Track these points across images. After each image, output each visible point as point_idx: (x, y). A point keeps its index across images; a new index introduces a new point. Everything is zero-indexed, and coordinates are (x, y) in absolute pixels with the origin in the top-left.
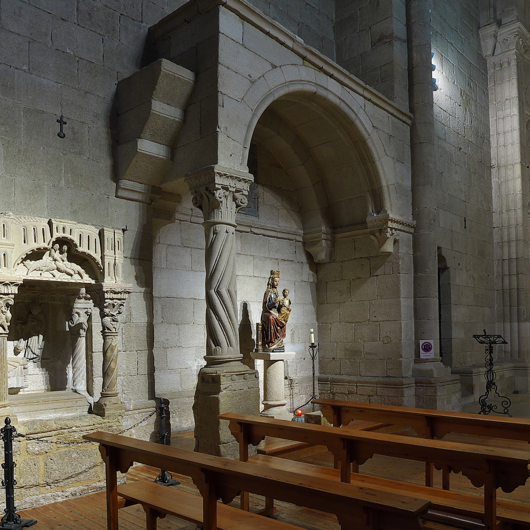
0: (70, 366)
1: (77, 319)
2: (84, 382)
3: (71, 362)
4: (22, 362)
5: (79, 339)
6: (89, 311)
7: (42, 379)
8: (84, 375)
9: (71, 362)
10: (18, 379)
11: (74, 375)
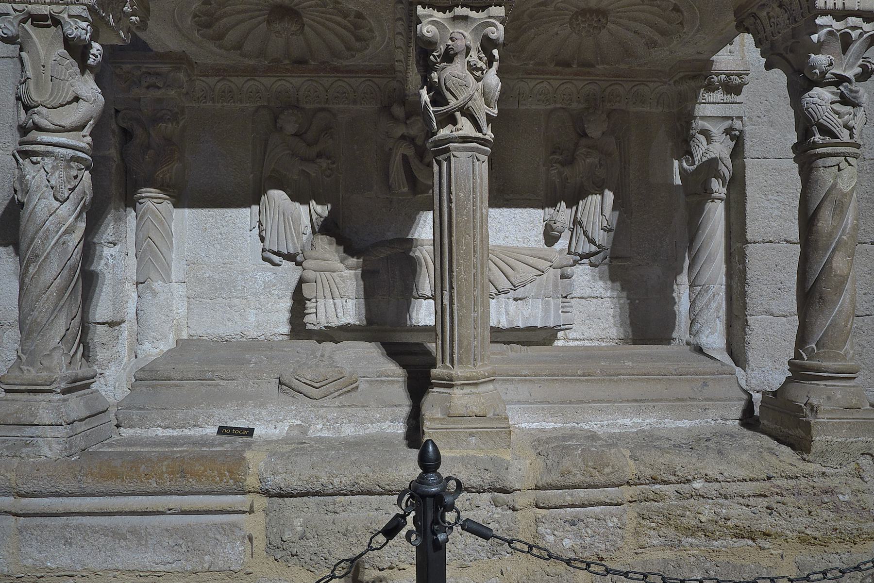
0: (683, 278)
1: (702, 150)
2: (720, 326)
3: (686, 270)
4: (557, 259)
5: (709, 205)
6: (738, 124)
7: (611, 311)
8: (720, 305)
9: (686, 270)
10: (548, 303)
11: (693, 303)
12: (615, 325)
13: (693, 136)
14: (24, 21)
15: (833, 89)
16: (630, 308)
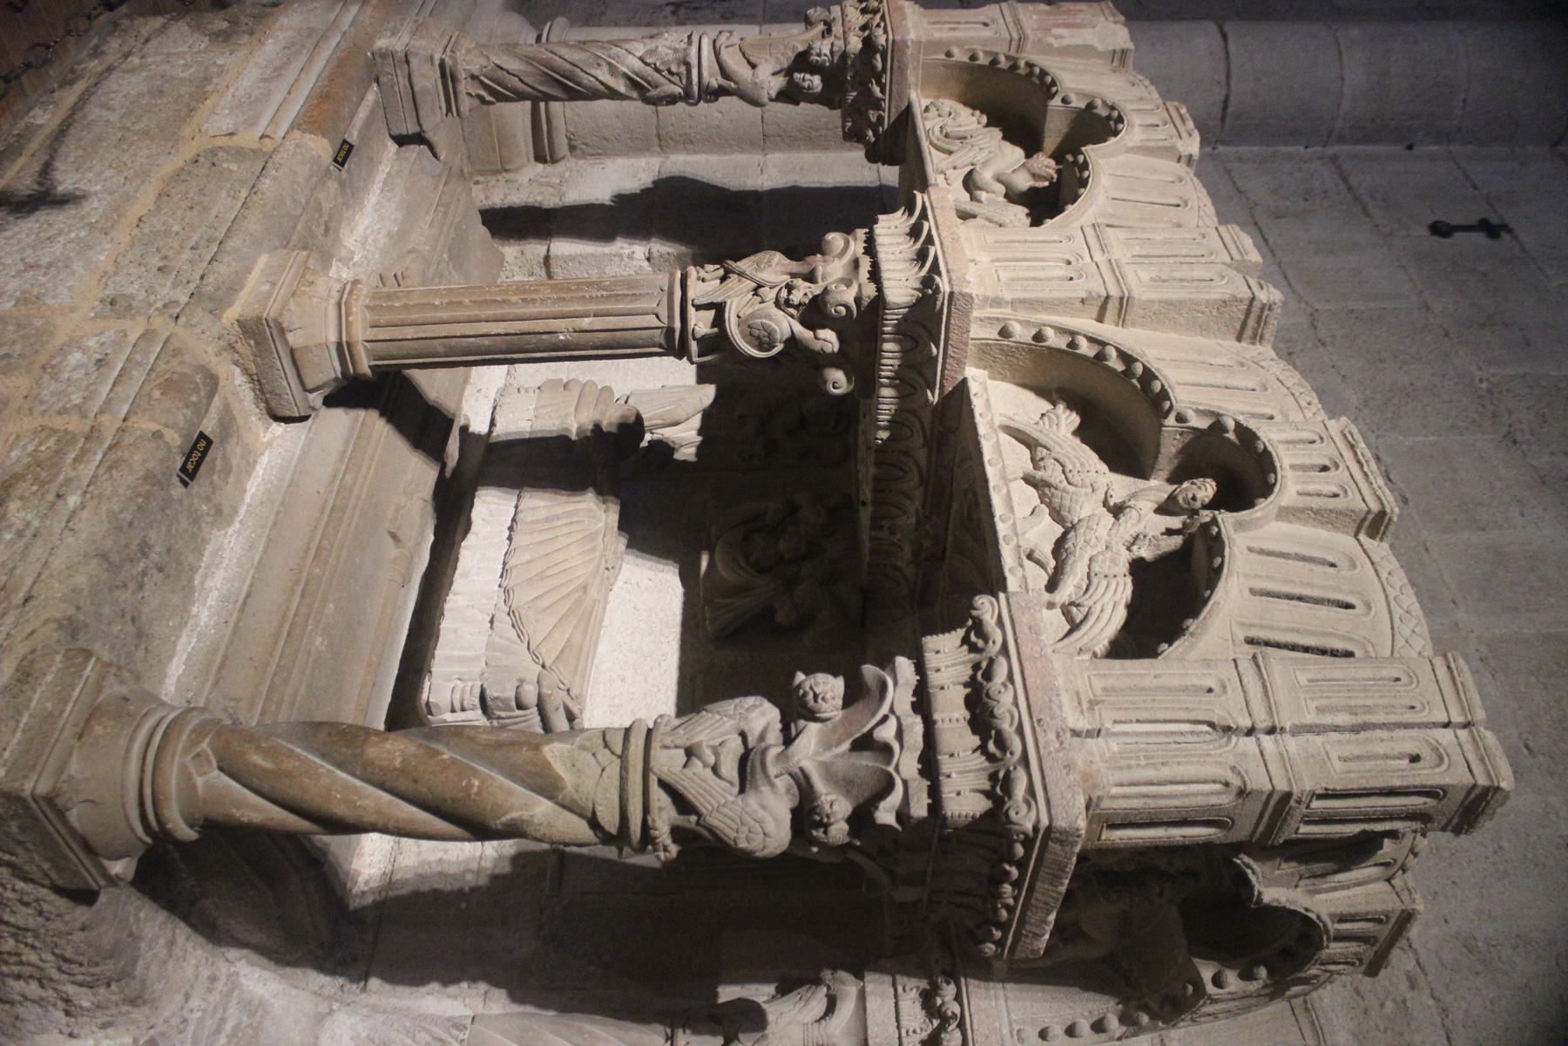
12: (424, 863)
13: (817, 982)
14: (826, 23)
15: (775, 736)
16: (451, 892)
